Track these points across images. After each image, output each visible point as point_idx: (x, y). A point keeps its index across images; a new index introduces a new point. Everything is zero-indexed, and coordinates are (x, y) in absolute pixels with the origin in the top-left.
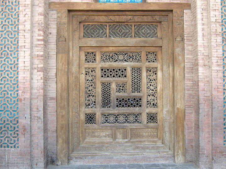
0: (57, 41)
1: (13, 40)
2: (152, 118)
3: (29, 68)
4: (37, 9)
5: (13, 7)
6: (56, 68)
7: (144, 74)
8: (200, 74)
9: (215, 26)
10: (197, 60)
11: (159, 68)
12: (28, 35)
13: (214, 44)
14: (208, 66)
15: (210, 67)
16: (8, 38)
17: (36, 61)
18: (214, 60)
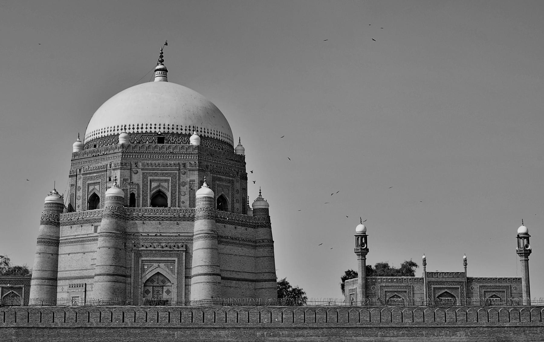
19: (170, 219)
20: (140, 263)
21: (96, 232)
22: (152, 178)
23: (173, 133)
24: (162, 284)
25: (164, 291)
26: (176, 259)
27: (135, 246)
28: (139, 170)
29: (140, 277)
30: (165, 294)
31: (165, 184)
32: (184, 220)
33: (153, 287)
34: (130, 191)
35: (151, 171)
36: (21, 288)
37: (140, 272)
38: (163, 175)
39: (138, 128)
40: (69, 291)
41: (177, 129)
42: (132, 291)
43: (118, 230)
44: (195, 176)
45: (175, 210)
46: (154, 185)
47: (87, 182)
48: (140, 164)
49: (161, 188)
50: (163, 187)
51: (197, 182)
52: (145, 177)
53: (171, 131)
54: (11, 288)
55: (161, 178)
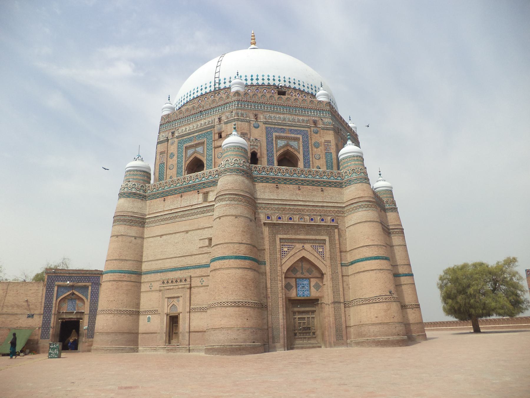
2: (314, 333)
19: (313, 183)
20: (278, 242)
21: (205, 199)
22: (277, 134)
23: (294, 89)
25: (312, 284)
26: (327, 238)
27: (268, 218)
28: (261, 124)
29: (279, 264)
30: (313, 289)
31: (294, 144)
32: (330, 186)
33: (296, 278)
35: (276, 126)
36: (86, 287)
38: (291, 131)
39: (252, 80)
40: (162, 288)
41: (299, 84)
43: (247, 192)
44: (330, 136)
45: (317, 172)
46: (281, 143)
47: (185, 145)
48: (262, 117)
49: (290, 149)
50: (291, 146)
51: (333, 143)
52: (268, 133)
53: (293, 86)
54: (72, 287)
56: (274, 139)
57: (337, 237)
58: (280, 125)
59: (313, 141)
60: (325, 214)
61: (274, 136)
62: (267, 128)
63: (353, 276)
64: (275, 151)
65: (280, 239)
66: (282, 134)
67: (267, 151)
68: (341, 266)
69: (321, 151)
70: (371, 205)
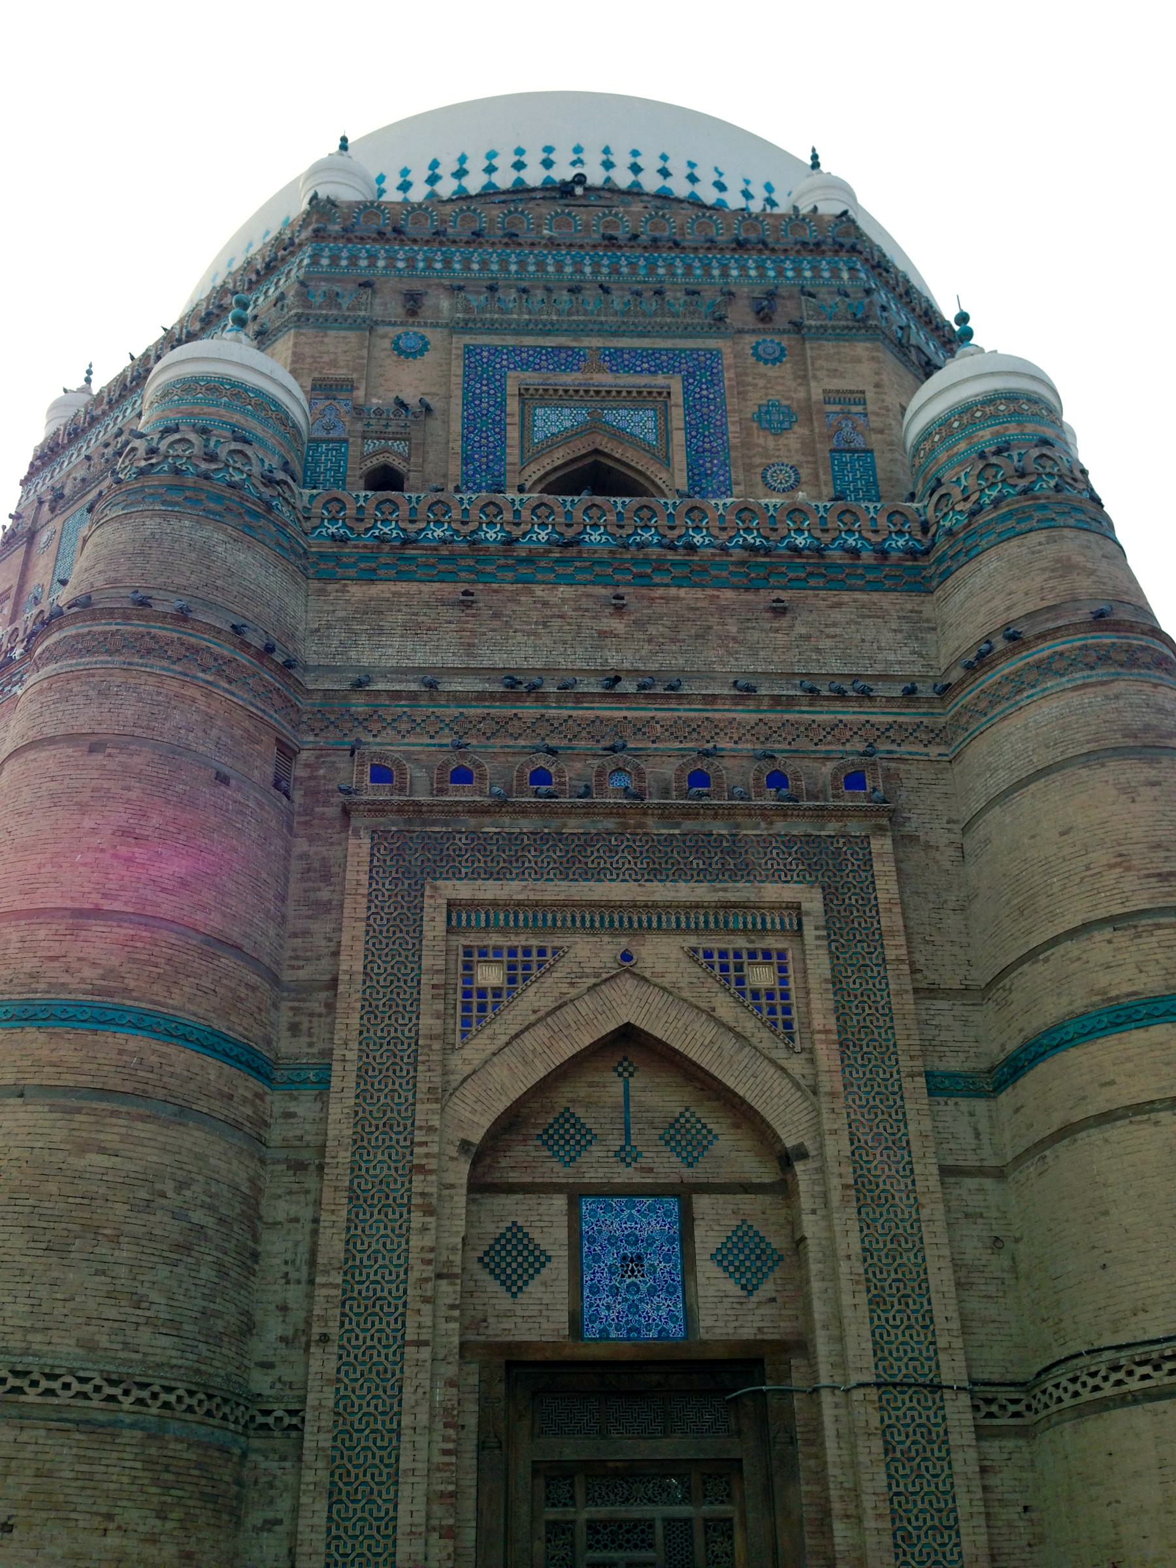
0: (481, 1447)
1: (385, 1453)
3: (422, 1529)
4: (442, 1370)
5: (389, 1367)
6: (474, 1524)
7: (699, 1540)
8: (837, 1540)
9: (862, 1410)
10: (828, 1500)
11: (736, 1520)
12: (422, 1441)
13: (863, 1458)
14: (858, 1520)
15: (860, 1520)
16: (374, 1449)
17: (438, 1510)
18: (868, 1502)
20: (434, 926)
22: (532, 378)
24: (667, 1167)
25: (707, 1239)
30: (712, 1283)
31: (642, 423)
33: (576, 1194)
34: (364, 457)
35: (529, 341)
37: (427, 1022)
38: (616, 360)
39: (433, 179)
42: (332, 1245)
49: (607, 446)
50: (618, 434)
52: (481, 372)
55: (605, 379)
56: (513, 406)
57: (886, 887)
58: (548, 333)
59: (756, 398)
60: (803, 744)
61: (512, 388)
62: (469, 351)
63: (1031, 1169)
64: (513, 455)
65: (451, 904)
66: (569, 379)
67: (466, 461)
68: (931, 1093)
69: (808, 447)
70: (1129, 649)
